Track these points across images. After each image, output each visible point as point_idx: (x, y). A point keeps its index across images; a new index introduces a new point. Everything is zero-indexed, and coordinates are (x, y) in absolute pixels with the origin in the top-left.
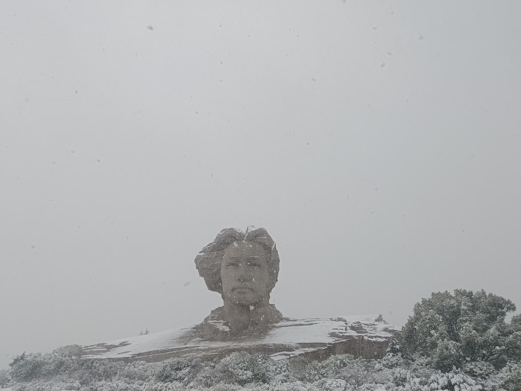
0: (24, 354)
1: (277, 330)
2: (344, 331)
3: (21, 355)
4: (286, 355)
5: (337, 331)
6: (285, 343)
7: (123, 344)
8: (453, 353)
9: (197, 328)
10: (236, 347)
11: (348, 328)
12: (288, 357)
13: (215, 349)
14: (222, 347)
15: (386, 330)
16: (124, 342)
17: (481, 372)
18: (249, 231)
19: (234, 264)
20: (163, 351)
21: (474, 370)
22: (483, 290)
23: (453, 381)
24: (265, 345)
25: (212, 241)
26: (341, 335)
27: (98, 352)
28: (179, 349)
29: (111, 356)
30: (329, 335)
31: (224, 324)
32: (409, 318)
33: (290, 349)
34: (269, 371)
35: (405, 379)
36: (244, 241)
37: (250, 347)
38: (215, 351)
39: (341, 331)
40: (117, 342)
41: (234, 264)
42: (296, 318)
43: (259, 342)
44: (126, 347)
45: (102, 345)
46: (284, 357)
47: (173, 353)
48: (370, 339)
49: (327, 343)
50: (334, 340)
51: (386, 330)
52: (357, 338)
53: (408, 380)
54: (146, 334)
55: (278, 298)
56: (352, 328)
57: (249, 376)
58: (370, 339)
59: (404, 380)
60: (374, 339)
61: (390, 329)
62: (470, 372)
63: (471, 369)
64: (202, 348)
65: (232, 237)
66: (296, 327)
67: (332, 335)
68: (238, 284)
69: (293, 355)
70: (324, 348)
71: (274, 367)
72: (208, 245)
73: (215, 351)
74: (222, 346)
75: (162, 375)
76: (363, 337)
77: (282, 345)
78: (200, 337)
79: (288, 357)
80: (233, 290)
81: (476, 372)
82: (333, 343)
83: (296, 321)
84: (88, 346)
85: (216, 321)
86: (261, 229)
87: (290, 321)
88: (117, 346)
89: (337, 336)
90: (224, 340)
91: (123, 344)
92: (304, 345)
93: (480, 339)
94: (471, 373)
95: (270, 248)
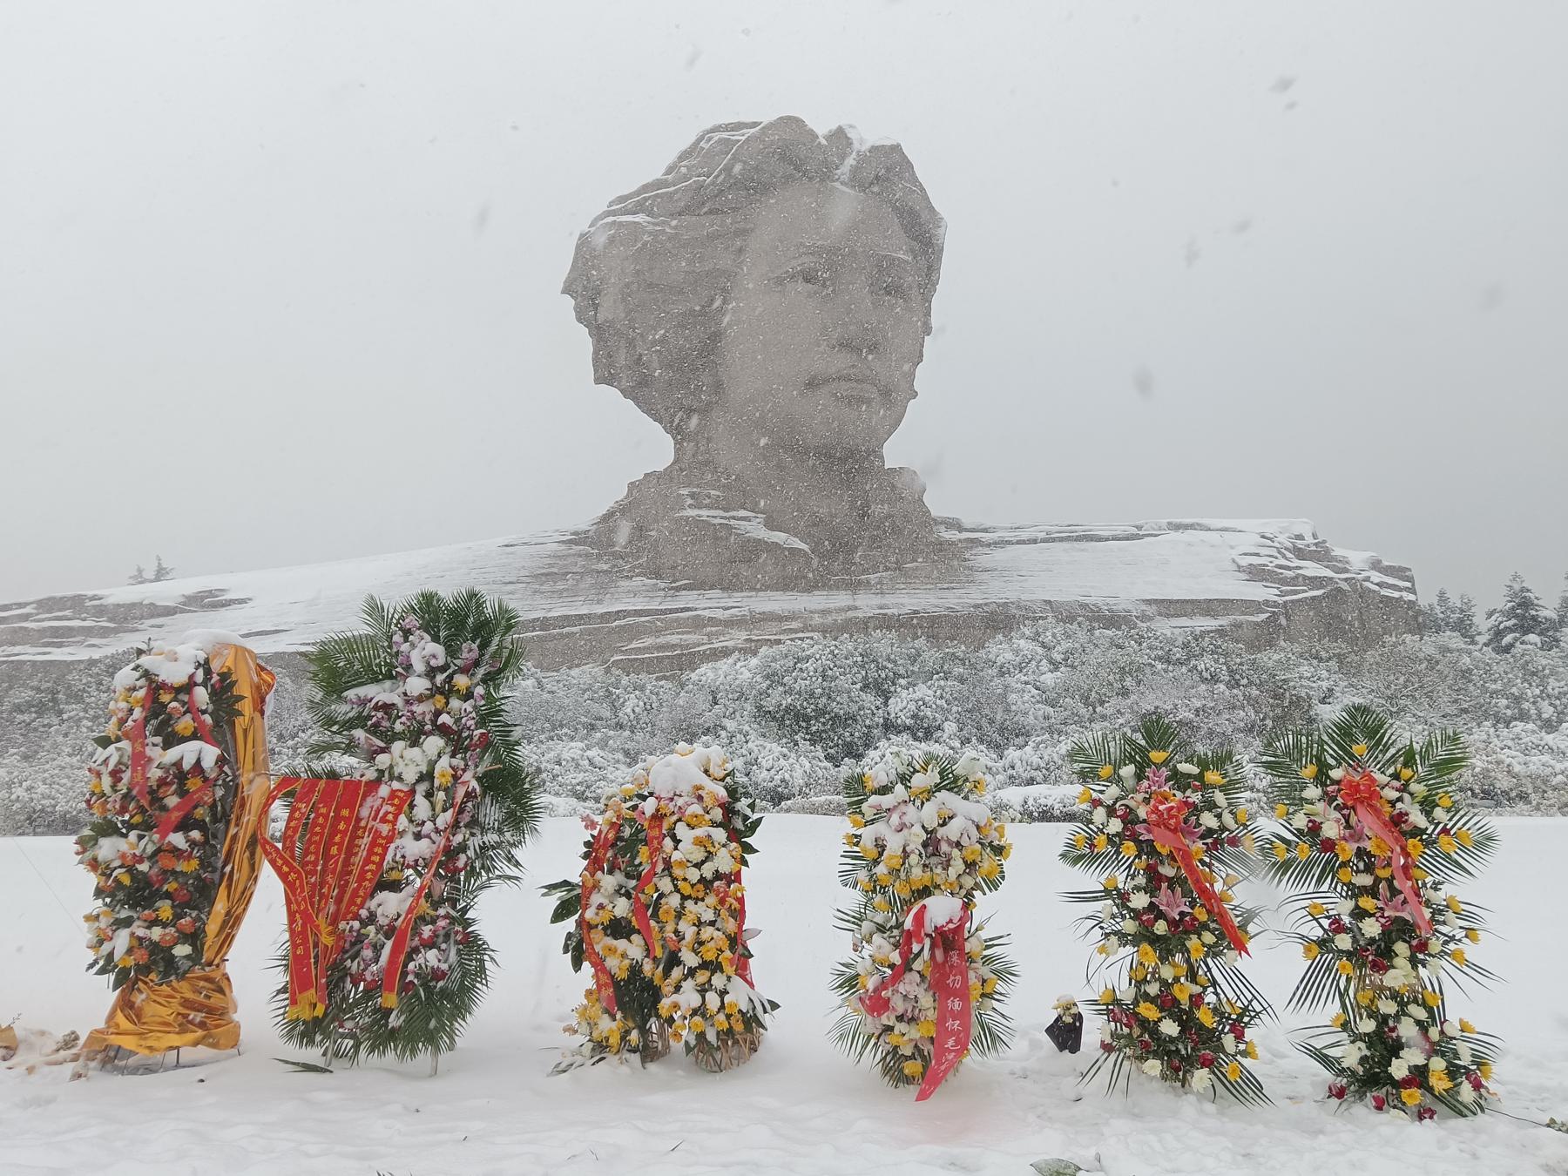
1: (999, 556)
6: (1087, 600)
7: (208, 601)
9: (579, 539)
10: (895, 611)
11: (1289, 555)
13: (787, 618)
14: (825, 612)
15: (1376, 565)
16: (210, 593)
18: (856, 146)
19: (819, 273)
25: (658, 173)
27: (55, 632)
28: (588, 617)
29: (248, 647)
31: (771, 525)
38: (794, 625)
42: (988, 524)
45: (76, 603)
47: (568, 635)
51: (1376, 565)
54: (157, 579)
56: (1300, 554)
60: (1384, 592)
61: (1386, 563)
64: (719, 614)
66: (1076, 544)
68: (841, 362)
72: (645, 188)
73: (794, 625)
74: (821, 607)
75: (821, 712)
80: (812, 384)
82: (1280, 600)
83: (985, 530)
85: (722, 513)
86: (897, 148)
87: (967, 530)
88: (170, 612)
91: (208, 601)
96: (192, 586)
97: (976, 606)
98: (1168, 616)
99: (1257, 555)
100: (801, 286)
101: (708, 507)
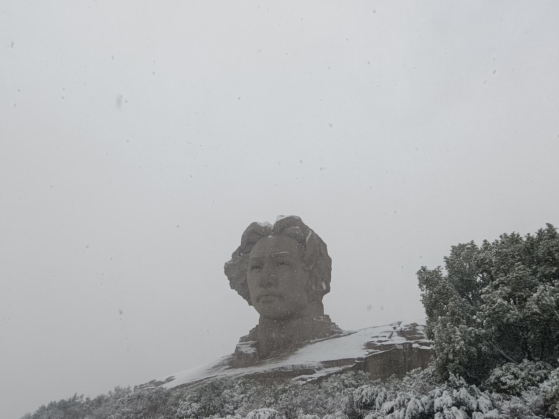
0: (75, 396)
2: (387, 339)
3: (72, 397)
4: (303, 380)
5: (375, 340)
8: (458, 347)
12: (305, 382)
16: (170, 378)
17: (513, 382)
19: (258, 267)
20: (190, 384)
21: (502, 379)
22: (549, 225)
23: (437, 403)
24: (283, 368)
26: (379, 344)
30: (364, 347)
32: (421, 298)
33: (310, 371)
34: (228, 402)
35: (373, 403)
36: (270, 236)
37: (265, 371)
39: (384, 339)
40: (163, 379)
41: (258, 267)
43: (281, 364)
44: (171, 382)
46: (301, 383)
48: (424, 347)
49: (356, 357)
50: (367, 353)
52: (402, 347)
53: (377, 404)
55: (331, 305)
56: (402, 333)
57: (194, 410)
58: (424, 347)
59: (369, 406)
62: (495, 385)
63: (498, 378)
65: (258, 234)
67: (369, 345)
69: (310, 380)
70: (351, 366)
71: (242, 396)
74: (237, 373)
76: (411, 344)
77: (302, 366)
78: (229, 365)
79: (305, 382)
81: (505, 384)
82: (364, 357)
84: (143, 385)
85: (245, 343)
88: (164, 383)
89: (376, 348)
90: (246, 366)
91: (169, 380)
92: (328, 364)
93: (514, 314)
94: (497, 386)
95: (305, 241)
96: (167, 377)
97: (273, 369)
98: (327, 367)
99: (377, 337)
100: (255, 270)
101: (245, 341)
